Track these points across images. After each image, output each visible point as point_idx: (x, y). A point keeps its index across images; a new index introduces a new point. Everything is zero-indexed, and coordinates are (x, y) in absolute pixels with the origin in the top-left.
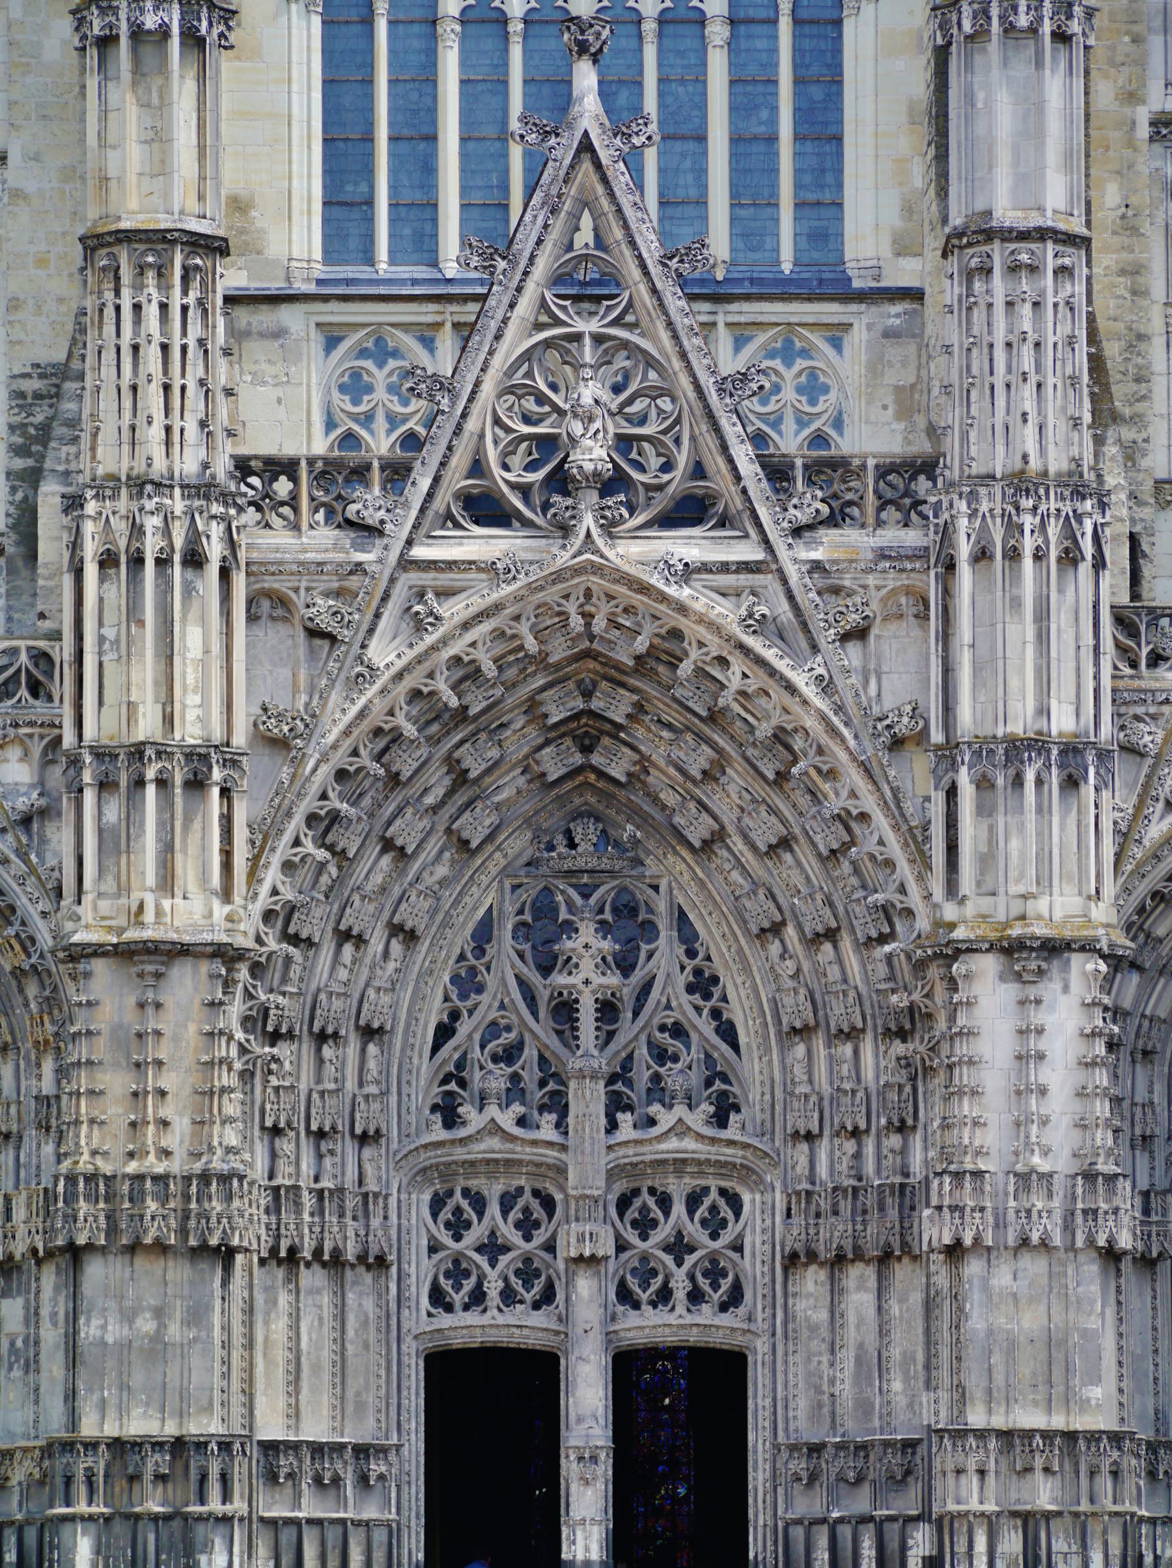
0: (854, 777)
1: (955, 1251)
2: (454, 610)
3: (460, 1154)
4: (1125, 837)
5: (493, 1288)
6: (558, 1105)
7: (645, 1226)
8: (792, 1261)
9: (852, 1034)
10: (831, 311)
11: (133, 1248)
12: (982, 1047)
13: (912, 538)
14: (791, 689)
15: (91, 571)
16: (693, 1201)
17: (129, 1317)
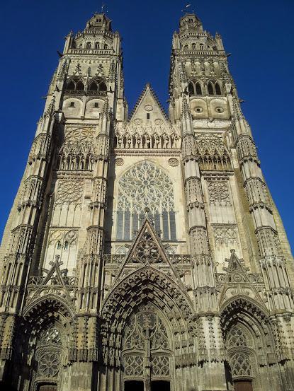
0: (183, 294)
1: (201, 363)
2: (130, 273)
3: (130, 351)
4: (220, 303)
5: (134, 372)
6: (143, 345)
7: (156, 363)
8: (177, 367)
9: (184, 332)
10: (175, 244)
11: (80, 361)
12: (204, 330)
13: (189, 264)
14: (174, 282)
15: (83, 266)
16: (162, 359)
17: (79, 372)
